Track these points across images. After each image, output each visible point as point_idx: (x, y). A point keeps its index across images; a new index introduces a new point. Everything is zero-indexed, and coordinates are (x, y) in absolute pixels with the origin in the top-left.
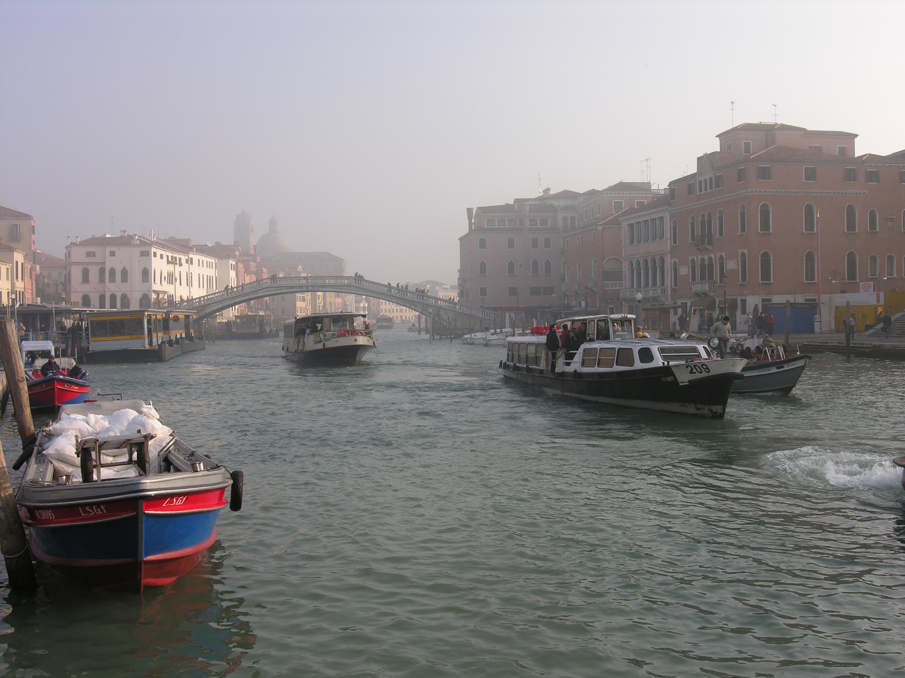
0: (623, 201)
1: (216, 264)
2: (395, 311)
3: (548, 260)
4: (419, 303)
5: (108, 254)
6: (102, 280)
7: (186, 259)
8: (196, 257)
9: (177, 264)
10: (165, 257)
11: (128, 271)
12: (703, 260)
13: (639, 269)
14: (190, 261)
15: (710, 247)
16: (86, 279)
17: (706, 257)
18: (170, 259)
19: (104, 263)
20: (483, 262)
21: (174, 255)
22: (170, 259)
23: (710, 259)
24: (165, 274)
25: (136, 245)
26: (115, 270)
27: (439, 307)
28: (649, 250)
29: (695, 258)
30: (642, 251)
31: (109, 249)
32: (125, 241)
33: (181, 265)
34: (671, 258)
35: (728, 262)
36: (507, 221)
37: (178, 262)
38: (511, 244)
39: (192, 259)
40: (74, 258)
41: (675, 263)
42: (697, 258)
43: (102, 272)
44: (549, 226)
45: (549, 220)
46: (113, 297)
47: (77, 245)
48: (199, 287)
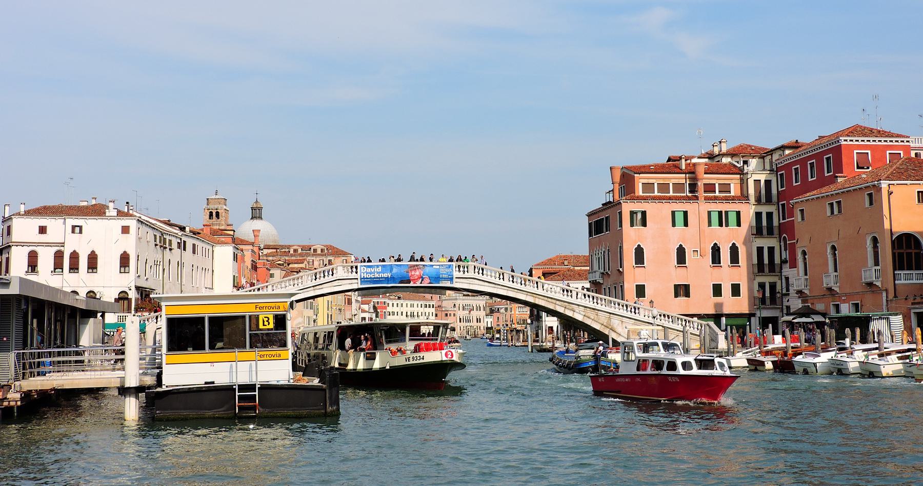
1: (213, 251)
3: (734, 244)
4: (578, 305)
5: (69, 229)
7: (178, 243)
8: (190, 242)
14: (182, 246)
19: (63, 245)
25: (111, 218)
27: (610, 313)
31: (71, 222)
37: (167, 246)
39: (185, 242)
40: (16, 236)
43: (59, 256)
44: (732, 194)
45: (732, 186)
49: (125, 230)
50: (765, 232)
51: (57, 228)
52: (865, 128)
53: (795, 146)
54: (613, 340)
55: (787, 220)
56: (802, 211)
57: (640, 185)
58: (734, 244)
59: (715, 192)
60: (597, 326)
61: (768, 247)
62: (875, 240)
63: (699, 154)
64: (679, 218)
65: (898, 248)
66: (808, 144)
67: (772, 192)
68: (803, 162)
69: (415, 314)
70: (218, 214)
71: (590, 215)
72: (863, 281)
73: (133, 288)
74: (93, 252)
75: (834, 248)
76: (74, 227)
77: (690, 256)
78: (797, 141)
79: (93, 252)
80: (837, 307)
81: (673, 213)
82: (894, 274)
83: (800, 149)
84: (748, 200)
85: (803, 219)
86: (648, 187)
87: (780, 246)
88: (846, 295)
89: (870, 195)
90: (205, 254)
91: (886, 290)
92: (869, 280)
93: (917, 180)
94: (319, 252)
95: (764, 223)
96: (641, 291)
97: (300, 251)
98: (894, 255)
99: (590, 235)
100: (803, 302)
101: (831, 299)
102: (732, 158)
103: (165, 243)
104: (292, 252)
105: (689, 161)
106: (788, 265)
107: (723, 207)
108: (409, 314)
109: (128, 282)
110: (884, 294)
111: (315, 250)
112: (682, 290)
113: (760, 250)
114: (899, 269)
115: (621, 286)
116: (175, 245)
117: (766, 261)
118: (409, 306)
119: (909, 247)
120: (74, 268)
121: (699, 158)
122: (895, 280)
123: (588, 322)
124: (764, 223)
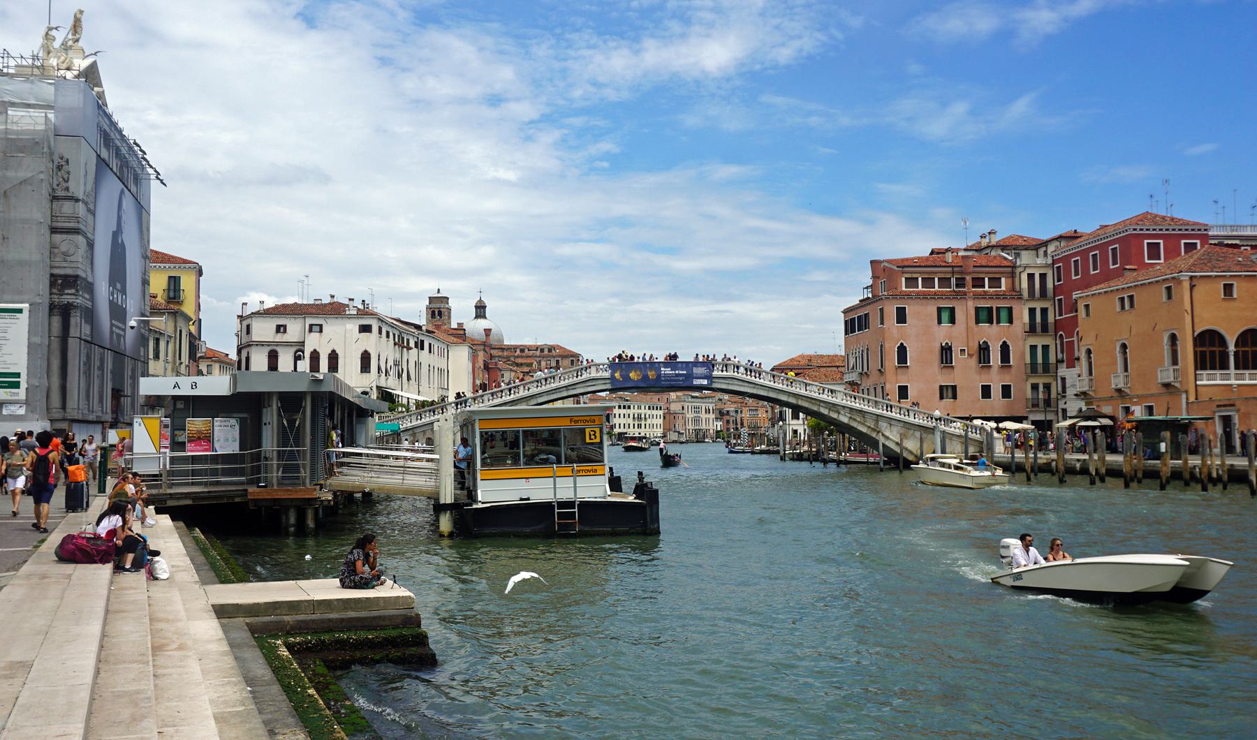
2: (632, 426)
3: (1004, 342)
4: (844, 407)
9: (404, 347)
11: (339, 356)
18: (397, 340)
20: (902, 344)
22: (397, 340)
24: (391, 363)
25: (350, 317)
26: (318, 353)
27: (878, 415)
32: (335, 310)
36: (936, 280)
39: (422, 342)
45: (1003, 280)
47: (261, 314)
50: (1039, 328)
51: (295, 329)
52: (1156, 216)
53: (1074, 236)
54: (883, 445)
55: (1064, 316)
56: (1087, 306)
57: (903, 279)
58: (1004, 342)
59: (984, 287)
60: (864, 430)
61: (1043, 346)
62: (1173, 338)
63: (964, 246)
64: (945, 316)
65: (1200, 346)
66: (1089, 234)
67: (1048, 286)
68: (1084, 253)
69: (643, 416)
70: (440, 314)
71: (845, 312)
72: (1160, 381)
73: (375, 389)
74: (334, 351)
75: (1124, 346)
76: (311, 326)
77: (957, 356)
78: (1075, 231)
79: (334, 351)
80: (1127, 410)
81: (939, 310)
82: (1196, 375)
83: (1079, 240)
84: (1021, 295)
85: (1088, 314)
86: (911, 282)
87: (1056, 344)
88: (1138, 397)
89: (1169, 289)
90: (441, 355)
91: (1187, 392)
92: (1166, 381)
93: (1224, 272)
94: (546, 352)
95: (1038, 319)
96: (903, 392)
97: (526, 350)
98: (1195, 352)
99: (846, 334)
100: (1087, 404)
101: (1120, 401)
102: (1003, 251)
103: (403, 342)
104: (518, 351)
105: (955, 254)
106: (1065, 364)
107: (994, 304)
108: (636, 416)
109: (370, 381)
110: (1184, 396)
111: (542, 350)
112: (950, 392)
113: (1033, 348)
114: (1202, 369)
115: (882, 387)
116: (412, 344)
117: (1040, 360)
118: (636, 407)
119: (1212, 344)
121: (965, 250)
122: (1196, 380)
123: (854, 424)
124: (1038, 319)
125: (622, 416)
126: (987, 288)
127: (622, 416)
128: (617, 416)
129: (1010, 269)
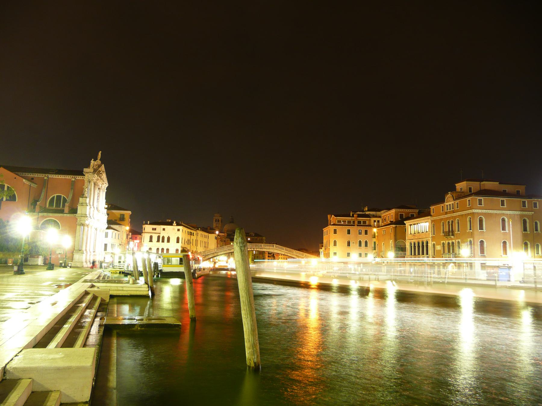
0: (404, 214)
3: (366, 240)
6: (158, 241)
9: (192, 235)
10: (187, 232)
12: (449, 243)
13: (415, 246)
14: (197, 234)
15: (452, 237)
16: (151, 241)
17: (450, 242)
21: (191, 232)
23: (453, 243)
24: (186, 240)
28: (420, 237)
29: (444, 242)
30: (416, 237)
33: (193, 235)
34: (432, 241)
35: (462, 244)
38: (349, 232)
41: (434, 245)
42: (446, 242)
43: (159, 237)
44: (367, 224)
45: (367, 222)
46: (163, 249)
48: (201, 246)
49: (179, 230)
58: (366, 240)
74: (169, 236)
79: (169, 236)
86: (339, 221)
90: (205, 237)
120: (163, 241)
125: (282, 258)
126: (362, 224)
127: (282, 258)
128: (281, 258)
129: (369, 219)
